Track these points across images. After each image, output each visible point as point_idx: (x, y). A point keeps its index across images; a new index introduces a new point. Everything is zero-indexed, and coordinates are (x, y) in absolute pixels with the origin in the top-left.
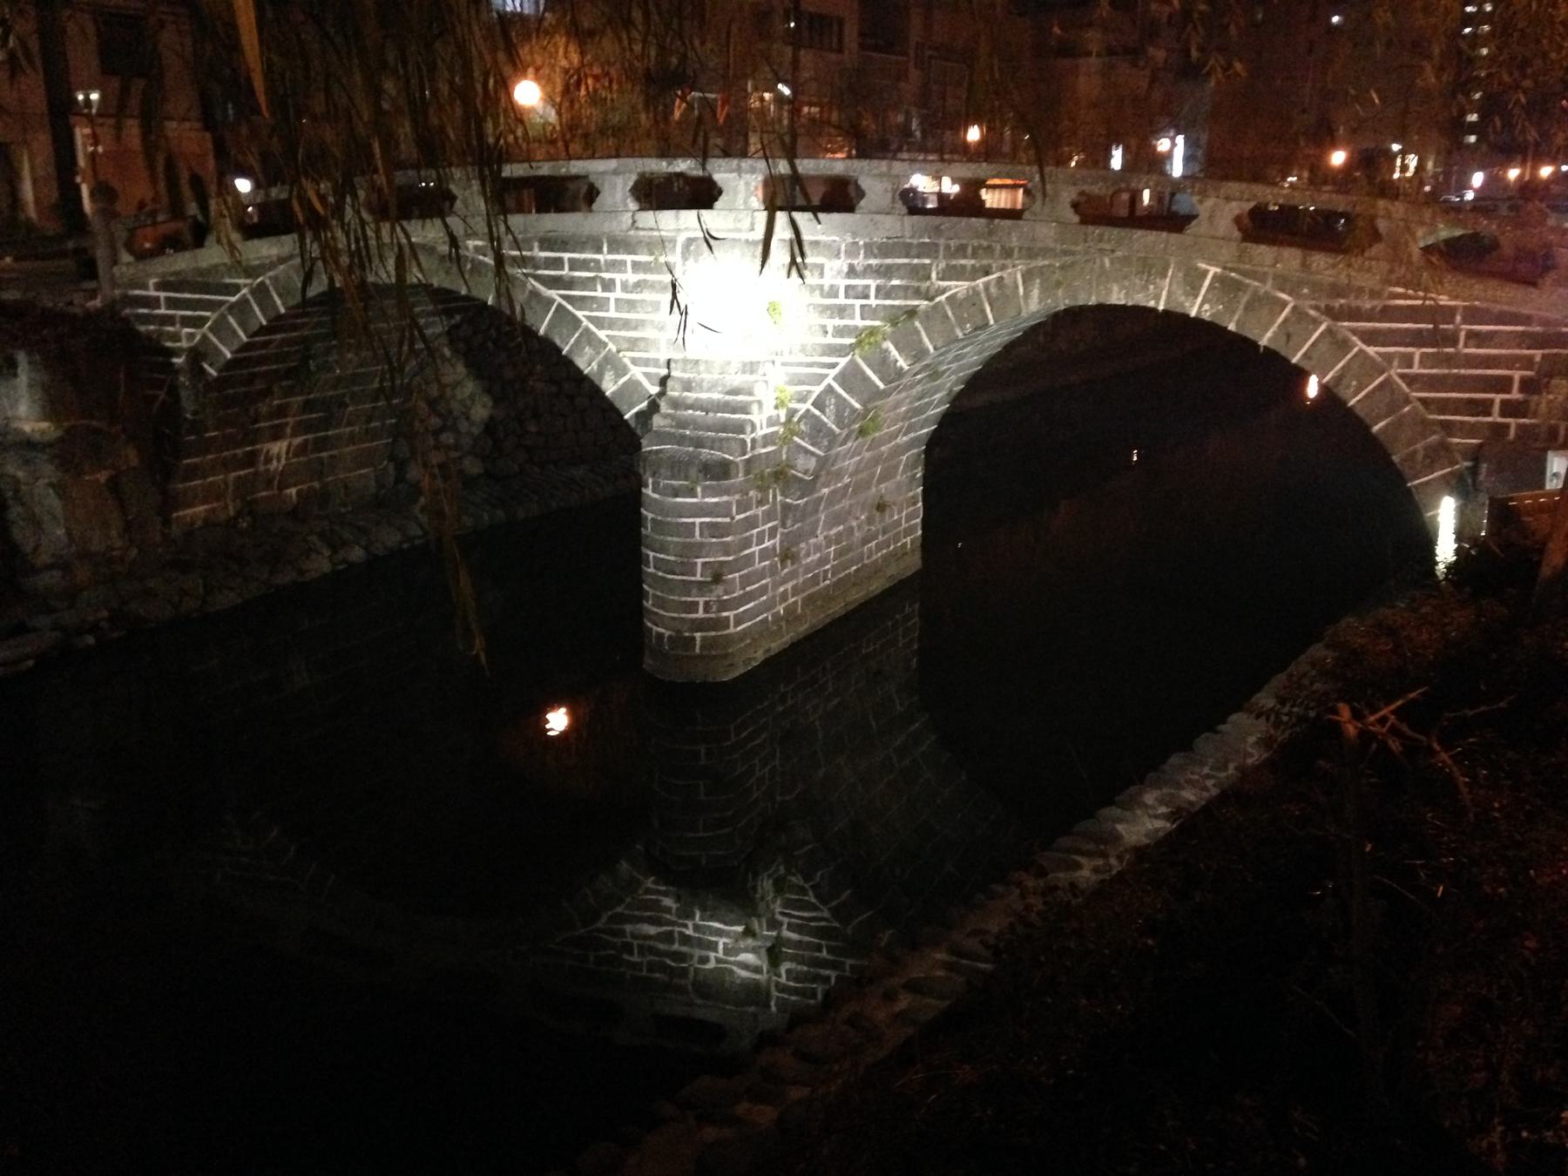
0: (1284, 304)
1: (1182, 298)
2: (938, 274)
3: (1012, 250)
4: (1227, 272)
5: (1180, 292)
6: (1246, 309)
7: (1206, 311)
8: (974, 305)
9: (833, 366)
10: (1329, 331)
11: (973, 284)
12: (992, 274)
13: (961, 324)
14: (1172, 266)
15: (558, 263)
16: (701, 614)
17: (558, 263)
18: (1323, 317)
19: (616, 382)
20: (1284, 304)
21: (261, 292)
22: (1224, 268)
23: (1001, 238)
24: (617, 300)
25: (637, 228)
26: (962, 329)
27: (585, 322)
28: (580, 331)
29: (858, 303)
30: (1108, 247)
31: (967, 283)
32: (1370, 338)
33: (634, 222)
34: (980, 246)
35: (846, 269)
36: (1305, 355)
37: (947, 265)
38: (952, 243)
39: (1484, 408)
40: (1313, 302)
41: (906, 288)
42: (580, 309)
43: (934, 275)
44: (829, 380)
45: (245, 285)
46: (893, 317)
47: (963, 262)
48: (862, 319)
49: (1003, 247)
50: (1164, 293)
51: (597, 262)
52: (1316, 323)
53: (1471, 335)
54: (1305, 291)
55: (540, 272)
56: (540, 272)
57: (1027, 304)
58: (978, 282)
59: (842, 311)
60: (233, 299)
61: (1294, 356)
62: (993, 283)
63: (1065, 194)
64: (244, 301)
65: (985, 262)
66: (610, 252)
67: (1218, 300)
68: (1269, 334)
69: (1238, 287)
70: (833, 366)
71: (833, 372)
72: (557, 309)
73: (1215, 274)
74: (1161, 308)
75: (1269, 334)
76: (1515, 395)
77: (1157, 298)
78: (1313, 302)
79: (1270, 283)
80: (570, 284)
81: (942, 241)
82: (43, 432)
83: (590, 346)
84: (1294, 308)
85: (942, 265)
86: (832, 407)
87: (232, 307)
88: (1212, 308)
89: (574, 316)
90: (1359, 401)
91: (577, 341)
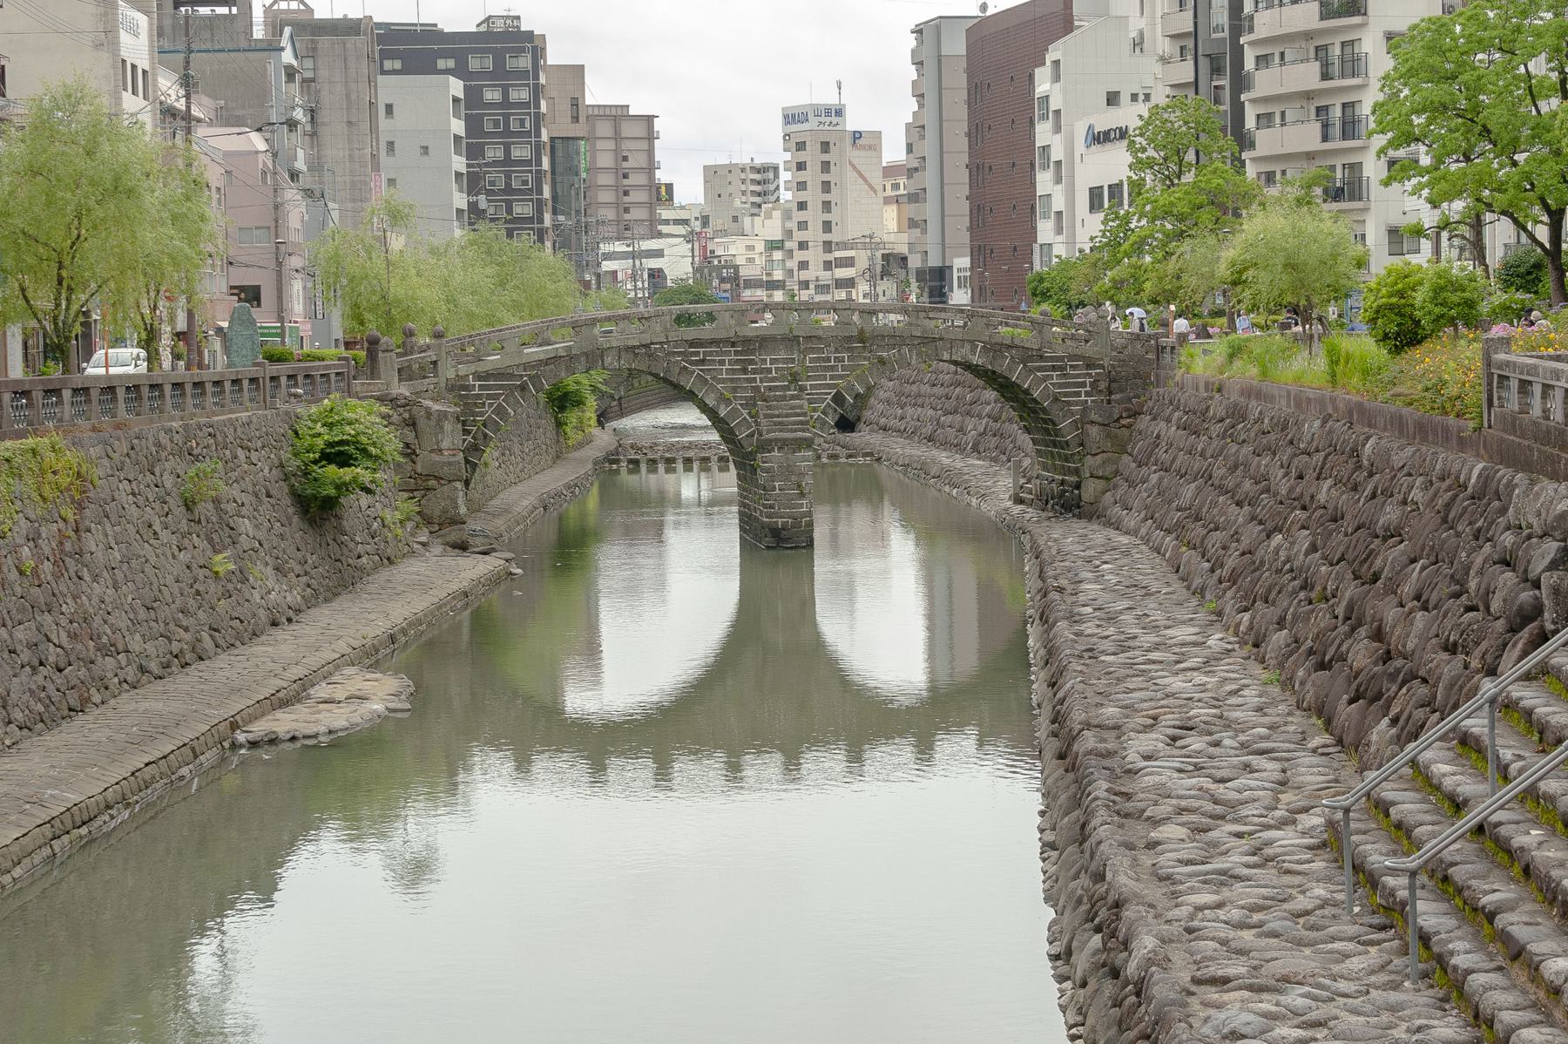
9: (830, 393)
39: (1078, 394)
45: (526, 375)
53: (1071, 366)
70: (830, 393)
71: (830, 397)
76: (1088, 389)
80: (702, 362)
91: (707, 391)
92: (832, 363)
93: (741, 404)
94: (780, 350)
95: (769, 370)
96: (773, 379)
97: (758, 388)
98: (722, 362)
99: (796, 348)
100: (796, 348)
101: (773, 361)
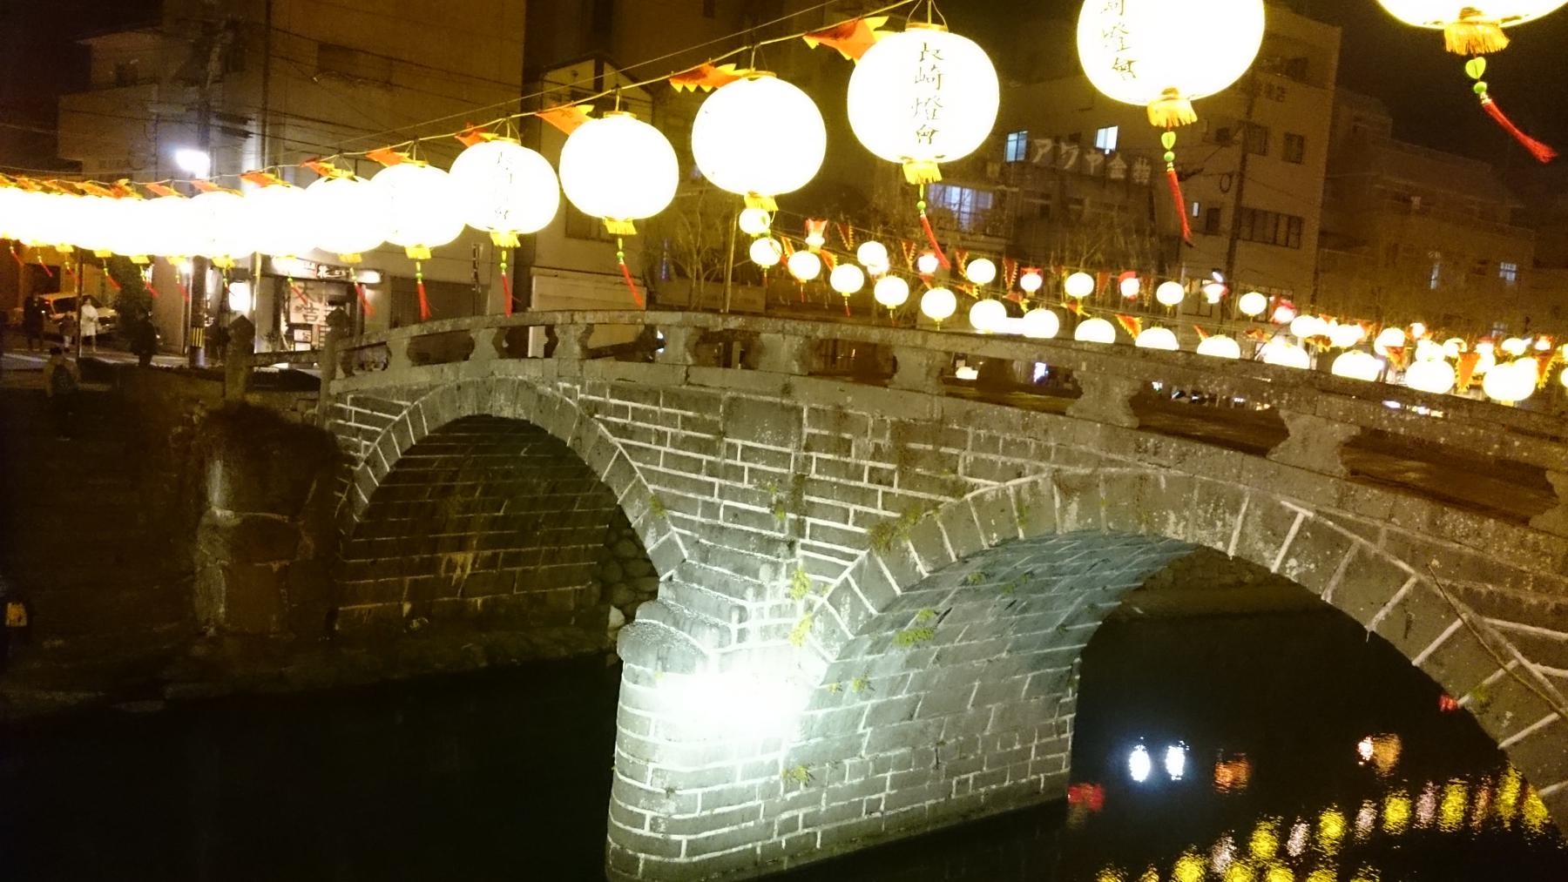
0: (1405, 577)
1: (1261, 545)
2: (965, 467)
3: (1049, 449)
4: (1322, 520)
5: (1257, 535)
6: (1347, 573)
7: (1292, 568)
8: (1003, 511)
9: (851, 558)
10: (1469, 628)
11: (1002, 485)
12: (1025, 476)
13: (988, 530)
14: (1247, 500)
15: (621, 411)
16: (646, 832)
17: (621, 411)
18: (1461, 606)
19: (657, 540)
20: (1405, 577)
21: (414, 413)
22: (1318, 512)
23: (1036, 433)
24: (666, 453)
25: (689, 384)
26: (988, 539)
27: (639, 474)
28: (634, 482)
29: (881, 489)
30: (1165, 463)
31: (996, 483)
32: (1537, 650)
33: (687, 376)
34: (1013, 442)
35: (872, 449)
36: (1431, 657)
37: (976, 459)
38: (982, 432)
40: (1448, 582)
41: (931, 480)
42: (636, 460)
43: (960, 469)
44: (846, 574)
46: (911, 508)
47: (993, 457)
48: (885, 509)
49: (1039, 446)
50: (1236, 534)
51: (654, 412)
52: (1453, 613)
54: (1435, 562)
55: (609, 418)
56: (609, 418)
57: (1063, 521)
58: (1008, 483)
59: (865, 496)
60: (397, 418)
61: (1416, 656)
62: (1026, 487)
63: (1117, 390)
64: (403, 421)
65: (1018, 461)
66: (664, 406)
67: (1309, 556)
68: (1381, 615)
69: (1337, 543)
71: (851, 565)
72: (618, 457)
73: (1306, 519)
74: (1231, 553)
75: (1381, 615)
77: (1226, 540)
78: (1448, 582)
79: (1382, 541)
81: (970, 430)
82: (227, 518)
83: (640, 498)
84: (1419, 584)
85: (970, 458)
86: (847, 606)
87: (396, 425)
88: (1299, 566)
89: (631, 466)
90: (1515, 744)
91: (630, 492)
92: (865, 484)
93: (683, 537)
94: (763, 430)
95: (737, 473)
96: (744, 495)
97: (710, 509)
98: (661, 438)
99: (794, 430)
100: (794, 430)
101: (748, 453)
